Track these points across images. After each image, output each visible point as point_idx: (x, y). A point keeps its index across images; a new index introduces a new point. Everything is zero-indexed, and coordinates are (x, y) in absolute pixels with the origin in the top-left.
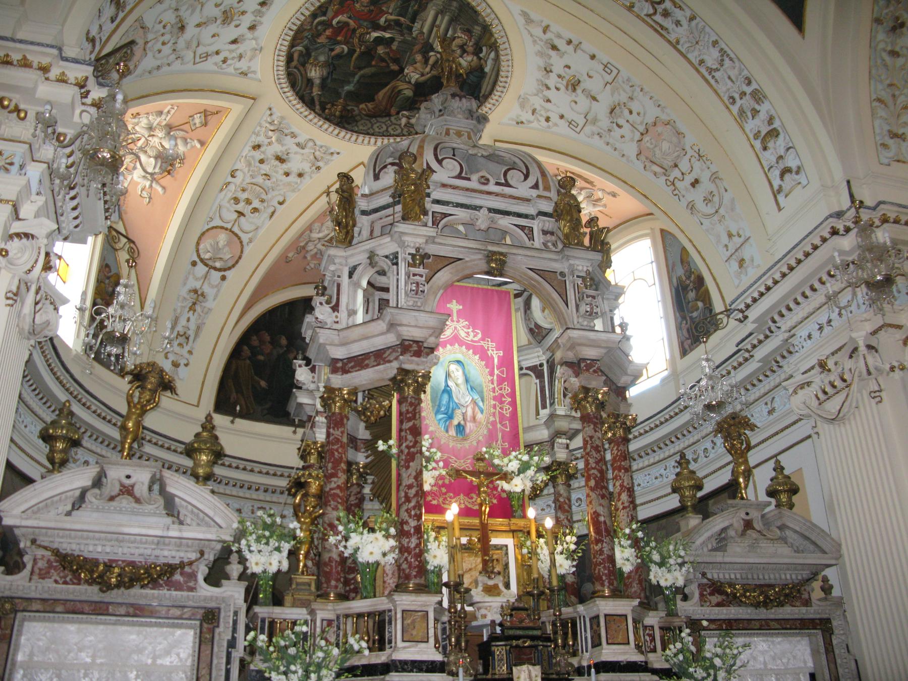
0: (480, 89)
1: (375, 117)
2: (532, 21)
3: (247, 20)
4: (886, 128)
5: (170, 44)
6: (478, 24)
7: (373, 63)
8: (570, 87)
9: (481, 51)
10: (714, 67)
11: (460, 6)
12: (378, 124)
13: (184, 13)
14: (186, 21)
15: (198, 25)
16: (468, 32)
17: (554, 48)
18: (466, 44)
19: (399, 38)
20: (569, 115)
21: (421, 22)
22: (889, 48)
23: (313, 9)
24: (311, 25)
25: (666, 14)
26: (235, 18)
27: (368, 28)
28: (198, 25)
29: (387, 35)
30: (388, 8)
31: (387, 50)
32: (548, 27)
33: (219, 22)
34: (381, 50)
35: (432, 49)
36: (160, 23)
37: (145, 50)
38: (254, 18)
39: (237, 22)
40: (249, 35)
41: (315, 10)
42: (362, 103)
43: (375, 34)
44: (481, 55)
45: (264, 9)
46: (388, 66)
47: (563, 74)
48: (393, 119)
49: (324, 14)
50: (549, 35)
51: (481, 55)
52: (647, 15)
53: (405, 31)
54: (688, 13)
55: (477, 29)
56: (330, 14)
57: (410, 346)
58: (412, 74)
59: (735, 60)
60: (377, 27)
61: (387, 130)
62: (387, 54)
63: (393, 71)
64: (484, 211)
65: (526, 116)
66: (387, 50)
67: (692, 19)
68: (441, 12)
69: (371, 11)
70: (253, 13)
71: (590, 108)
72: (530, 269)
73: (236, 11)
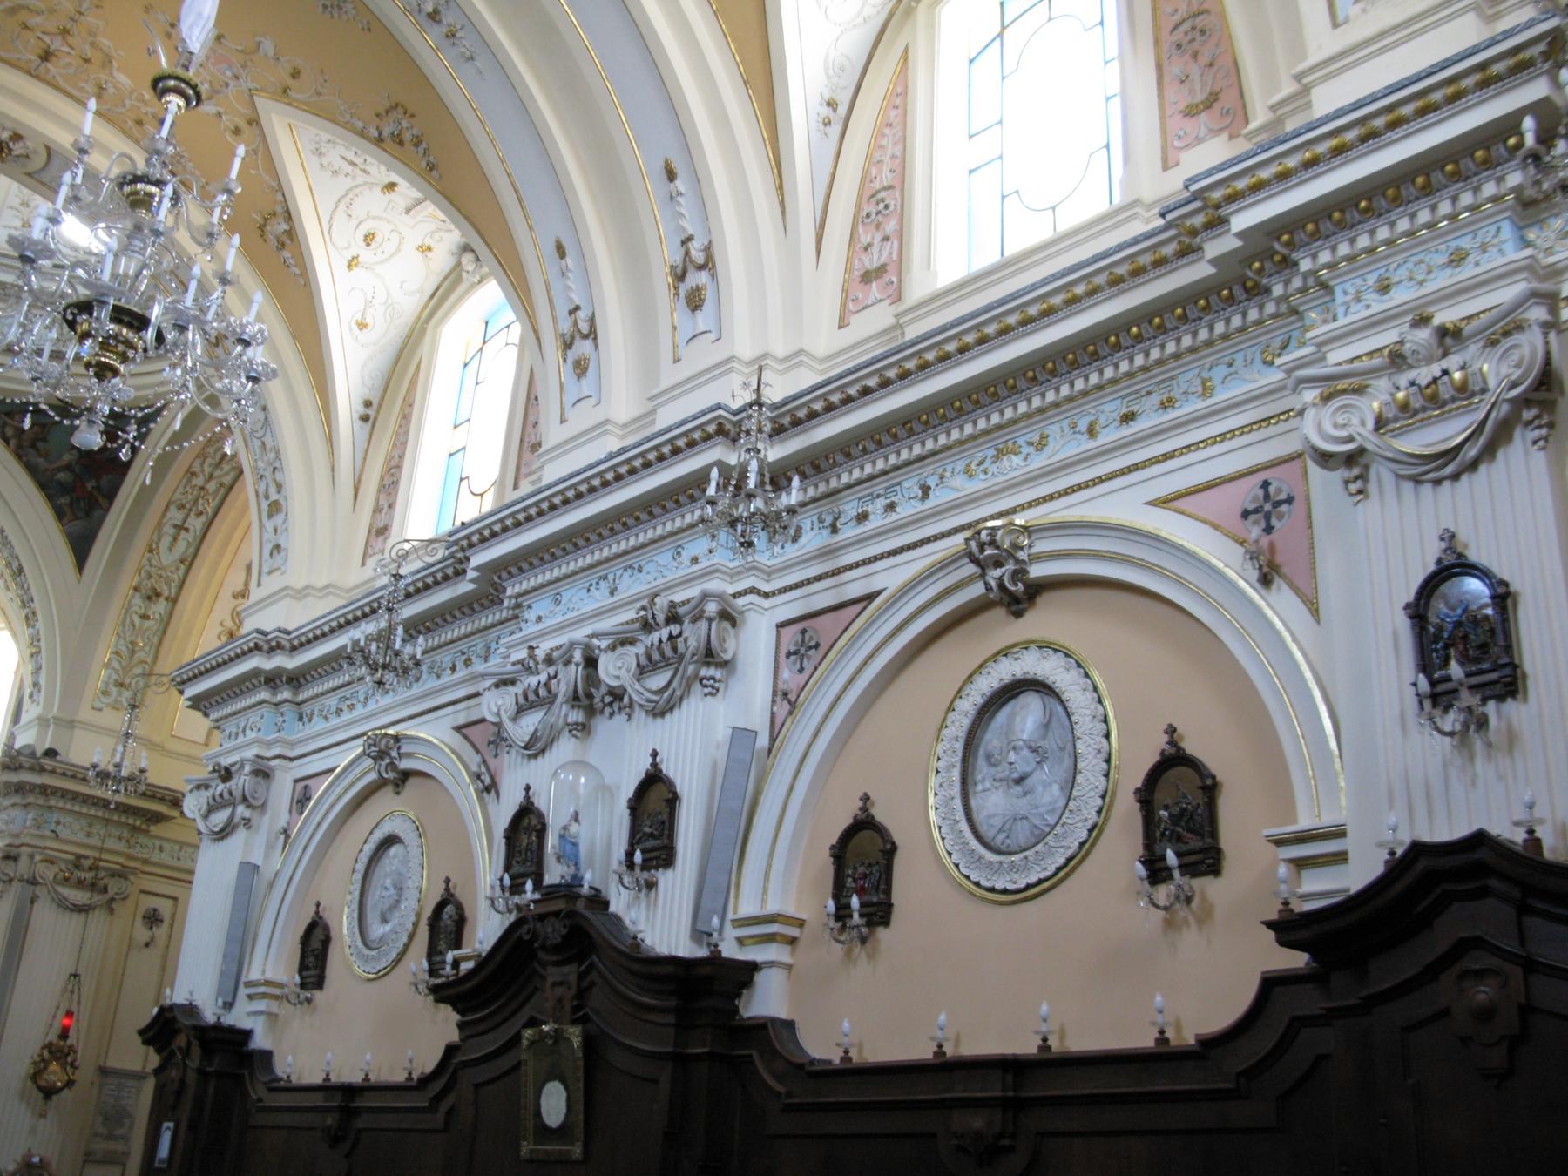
4: (114, 676)
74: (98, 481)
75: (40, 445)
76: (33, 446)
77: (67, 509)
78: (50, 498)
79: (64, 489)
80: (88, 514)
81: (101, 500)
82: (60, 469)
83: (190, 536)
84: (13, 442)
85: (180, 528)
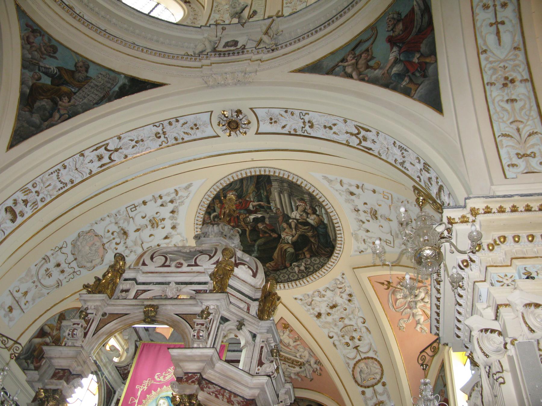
0: (329, 236)
1: (278, 270)
2: (331, 181)
3: (168, 223)
5: (122, 243)
6: (305, 193)
7: (261, 235)
8: (373, 217)
9: (317, 211)
10: (402, 161)
11: (289, 185)
12: (282, 275)
13: (125, 226)
14: (126, 230)
15: (138, 230)
16: (302, 200)
17: (352, 194)
18: (305, 209)
19: (267, 216)
20: (384, 237)
21: (273, 202)
22: (506, 98)
23: (205, 209)
24: (210, 219)
25: (365, 139)
26: (159, 223)
27: (246, 214)
28: (138, 230)
29: (260, 216)
30: (250, 198)
31: (265, 225)
32: (341, 181)
33: (149, 227)
34: (261, 226)
35: (289, 218)
36: (109, 232)
37: (104, 249)
38: (172, 222)
39: (163, 226)
40: (173, 232)
41: (207, 210)
42: (266, 263)
43: (252, 217)
44: (317, 213)
45: (175, 215)
46: (271, 236)
47: (366, 210)
48: (289, 269)
49: (214, 211)
50: (345, 186)
51: (317, 213)
52: (358, 145)
53: (268, 210)
54: (374, 132)
55: (306, 197)
56: (218, 210)
57: (59, 373)
58: (287, 237)
59: (408, 149)
60: (251, 212)
61: (289, 278)
62: (265, 227)
63: (275, 238)
64: (173, 285)
65: (362, 246)
66: (265, 225)
67: (378, 134)
68: (280, 193)
69: (240, 203)
70: (169, 218)
71: (390, 227)
72: (177, 314)
73: (158, 219)
74: (419, 51)
75: (371, 63)
76: (368, 67)
77: (410, 86)
78: (395, 89)
79: (400, 76)
80: (425, 76)
81: (428, 60)
82: (392, 67)
83: (508, 26)
84: (354, 75)
85: (497, 24)
